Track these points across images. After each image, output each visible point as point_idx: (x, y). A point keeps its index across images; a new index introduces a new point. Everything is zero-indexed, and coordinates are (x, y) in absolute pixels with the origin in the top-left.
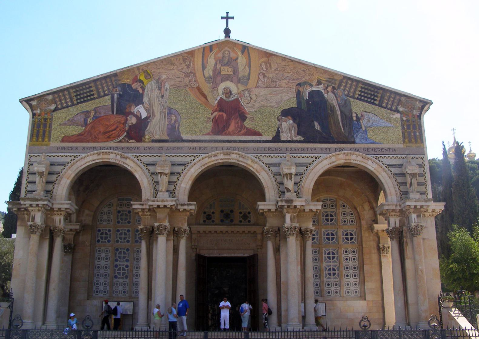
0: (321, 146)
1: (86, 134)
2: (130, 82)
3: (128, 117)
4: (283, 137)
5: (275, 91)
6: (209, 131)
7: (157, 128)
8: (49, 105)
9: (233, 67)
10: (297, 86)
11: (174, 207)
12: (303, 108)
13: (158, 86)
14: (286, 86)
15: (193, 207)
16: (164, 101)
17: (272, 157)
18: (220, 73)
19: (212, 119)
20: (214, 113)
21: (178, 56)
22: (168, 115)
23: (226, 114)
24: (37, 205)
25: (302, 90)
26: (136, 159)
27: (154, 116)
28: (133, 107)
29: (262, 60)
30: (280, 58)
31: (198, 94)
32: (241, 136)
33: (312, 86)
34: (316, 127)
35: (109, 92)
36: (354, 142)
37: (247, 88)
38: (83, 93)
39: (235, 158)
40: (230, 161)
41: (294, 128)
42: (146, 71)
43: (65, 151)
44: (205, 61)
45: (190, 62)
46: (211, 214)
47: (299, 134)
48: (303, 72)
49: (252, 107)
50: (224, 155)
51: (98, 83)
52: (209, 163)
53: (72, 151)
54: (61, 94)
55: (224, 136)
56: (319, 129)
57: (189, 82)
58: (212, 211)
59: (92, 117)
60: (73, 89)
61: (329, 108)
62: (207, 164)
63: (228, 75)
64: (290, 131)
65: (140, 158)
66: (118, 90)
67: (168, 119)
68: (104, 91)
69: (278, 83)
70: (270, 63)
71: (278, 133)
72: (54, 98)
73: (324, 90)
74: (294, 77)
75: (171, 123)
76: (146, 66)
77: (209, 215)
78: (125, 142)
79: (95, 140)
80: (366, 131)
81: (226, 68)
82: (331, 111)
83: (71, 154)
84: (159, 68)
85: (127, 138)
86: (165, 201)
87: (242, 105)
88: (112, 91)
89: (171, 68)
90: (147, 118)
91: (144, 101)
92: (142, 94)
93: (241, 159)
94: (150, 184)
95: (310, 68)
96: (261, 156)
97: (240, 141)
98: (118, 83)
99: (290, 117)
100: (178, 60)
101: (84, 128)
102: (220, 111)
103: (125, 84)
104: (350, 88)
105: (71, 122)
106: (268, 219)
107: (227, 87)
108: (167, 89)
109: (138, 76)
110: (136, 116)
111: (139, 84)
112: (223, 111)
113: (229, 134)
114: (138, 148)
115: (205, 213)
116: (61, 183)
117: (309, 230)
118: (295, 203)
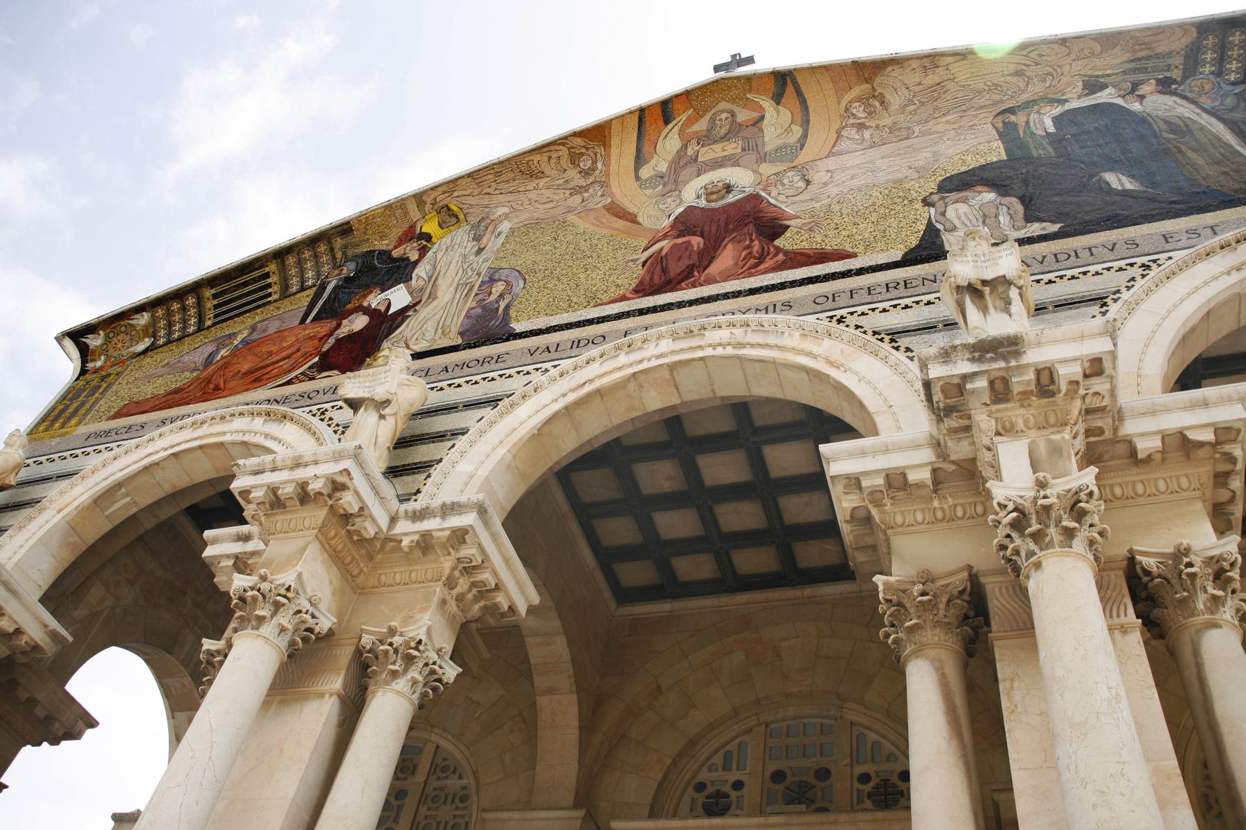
0: (1162, 229)
1: (192, 387)
2: (388, 245)
3: (345, 322)
5: (909, 147)
7: (430, 326)
8: (135, 343)
9: (743, 138)
10: (1000, 118)
11: (348, 501)
12: (1035, 153)
13: (475, 235)
14: (954, 126)
15: (467, 519)
16: (481, 260)
17: (907, 307)
18: (696, 160)
19: (643, 260)
20: (652, 245)
21: (553, 148)
22: (480, 286)
23: (702, 237)
25: (1025, 119)
26: (315, 421)
27: (430, 300)
28: (371, 296)
29: (848, 97)
30: (915, 64)
31: (607, 218)
32: (761, 277)
33: (1066, 101)
34: (1115, 185)
35: (318, 279)
37: (794, 164)
38: (240, 297)
39: (725, 340)
40: (699, 354)
41: (1005, 209)
42: (447, 206)
43: (104, 440)
44: (646, 148)
45: (595, 162)
46: (727, 789)
47: (1029, 218)
48: (1015, 78)
49: (812, 199)
50: (673, 340)
51: (291, 260)
52: (601, 376)
54: (176, 306)
55: (684, 291)
56: (1129, 185)
57: (583, 201)
58: (734, 776)
59: (236, 342)
60: (212, 288)
61: (1164, 127)
62: (591, 381)
63: (725, 157)
65: (328, 415)
66: (344, 272)
67: (477, 294)
68: (303, 282)
69: (916, 129)
70: (880, 94)
72: (154, 322)
73: (1123, 97)
74: (982, 102)
75: (489, 300)
76: (444, 193)
77: (719, 795)
78: (301, 381)
81: (717, 147)
82: (1172, 131)
84: (488, 194)
85: (315, 370)
86: (306, 466)
87: (771, 204)
88: (327, 277)
89: (531, 188)
90: (407, 308)
91: (414, 275)
92: (416, 263)
93: (752, 338)
95: (1040, 56)
96: (852, 313)
97: (752, 292)
98: (350, 253)
99: (979, 188)
100: (552, 161)
102: (678, 237)
103: (374, 251)
106: (901, 543)
107: (716, 181)
108: (499, 234)
109: (419, 225)
110: (372, 313)
111: (415, 244)
112: (694, 234)
113: (711, 281)
115: (701, 787)
116: (29, 527)
117: (1197, 560)
118: (1034, 356)
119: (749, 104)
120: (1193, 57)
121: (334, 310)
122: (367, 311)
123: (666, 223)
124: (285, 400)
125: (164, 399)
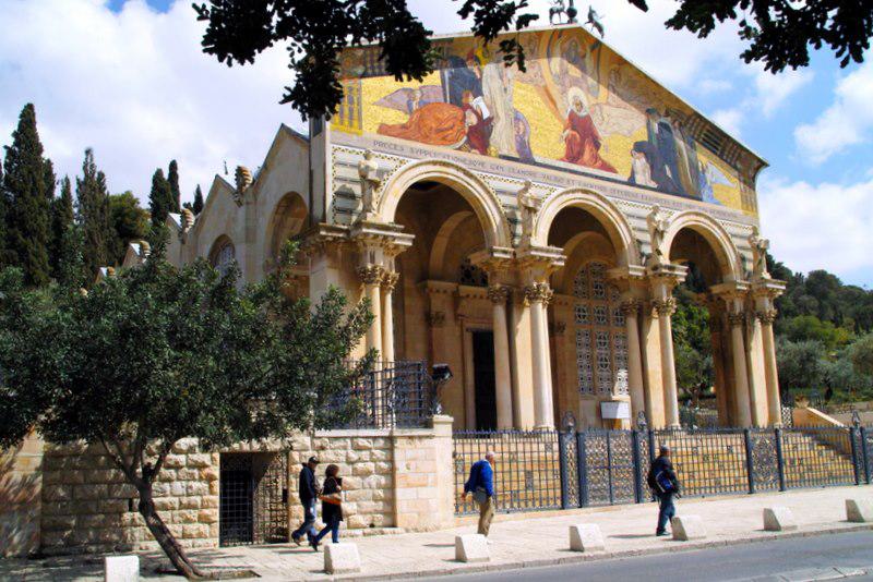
4: (639, 179)
6: (563, 155)
24: (385, 237)
28: (471, 97)
36: (701, 200)
53: (395, 152)
64: (644, 171)
71: (633, 173)
79: (425, 139)
80: (710, 187)
83: (395, 157)
90: (490, 119)
92: (481, 79)
94: (504, 222)
97: (597, 177)
98: (450, 54)
101: (408, 116)
102: (573, 129)
104: (696, 128)
105: (389, 101)
110: (476, 113)
113: (584, 164)
114: (482, 164)
119: (584, 47)
120: (689, 118)
121: (457, 100)
122: (471, 108)
123: (566, 116)
124: (464, 161)
125: (400, 131)
